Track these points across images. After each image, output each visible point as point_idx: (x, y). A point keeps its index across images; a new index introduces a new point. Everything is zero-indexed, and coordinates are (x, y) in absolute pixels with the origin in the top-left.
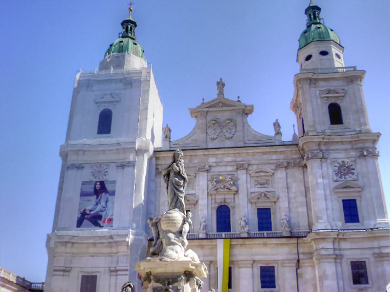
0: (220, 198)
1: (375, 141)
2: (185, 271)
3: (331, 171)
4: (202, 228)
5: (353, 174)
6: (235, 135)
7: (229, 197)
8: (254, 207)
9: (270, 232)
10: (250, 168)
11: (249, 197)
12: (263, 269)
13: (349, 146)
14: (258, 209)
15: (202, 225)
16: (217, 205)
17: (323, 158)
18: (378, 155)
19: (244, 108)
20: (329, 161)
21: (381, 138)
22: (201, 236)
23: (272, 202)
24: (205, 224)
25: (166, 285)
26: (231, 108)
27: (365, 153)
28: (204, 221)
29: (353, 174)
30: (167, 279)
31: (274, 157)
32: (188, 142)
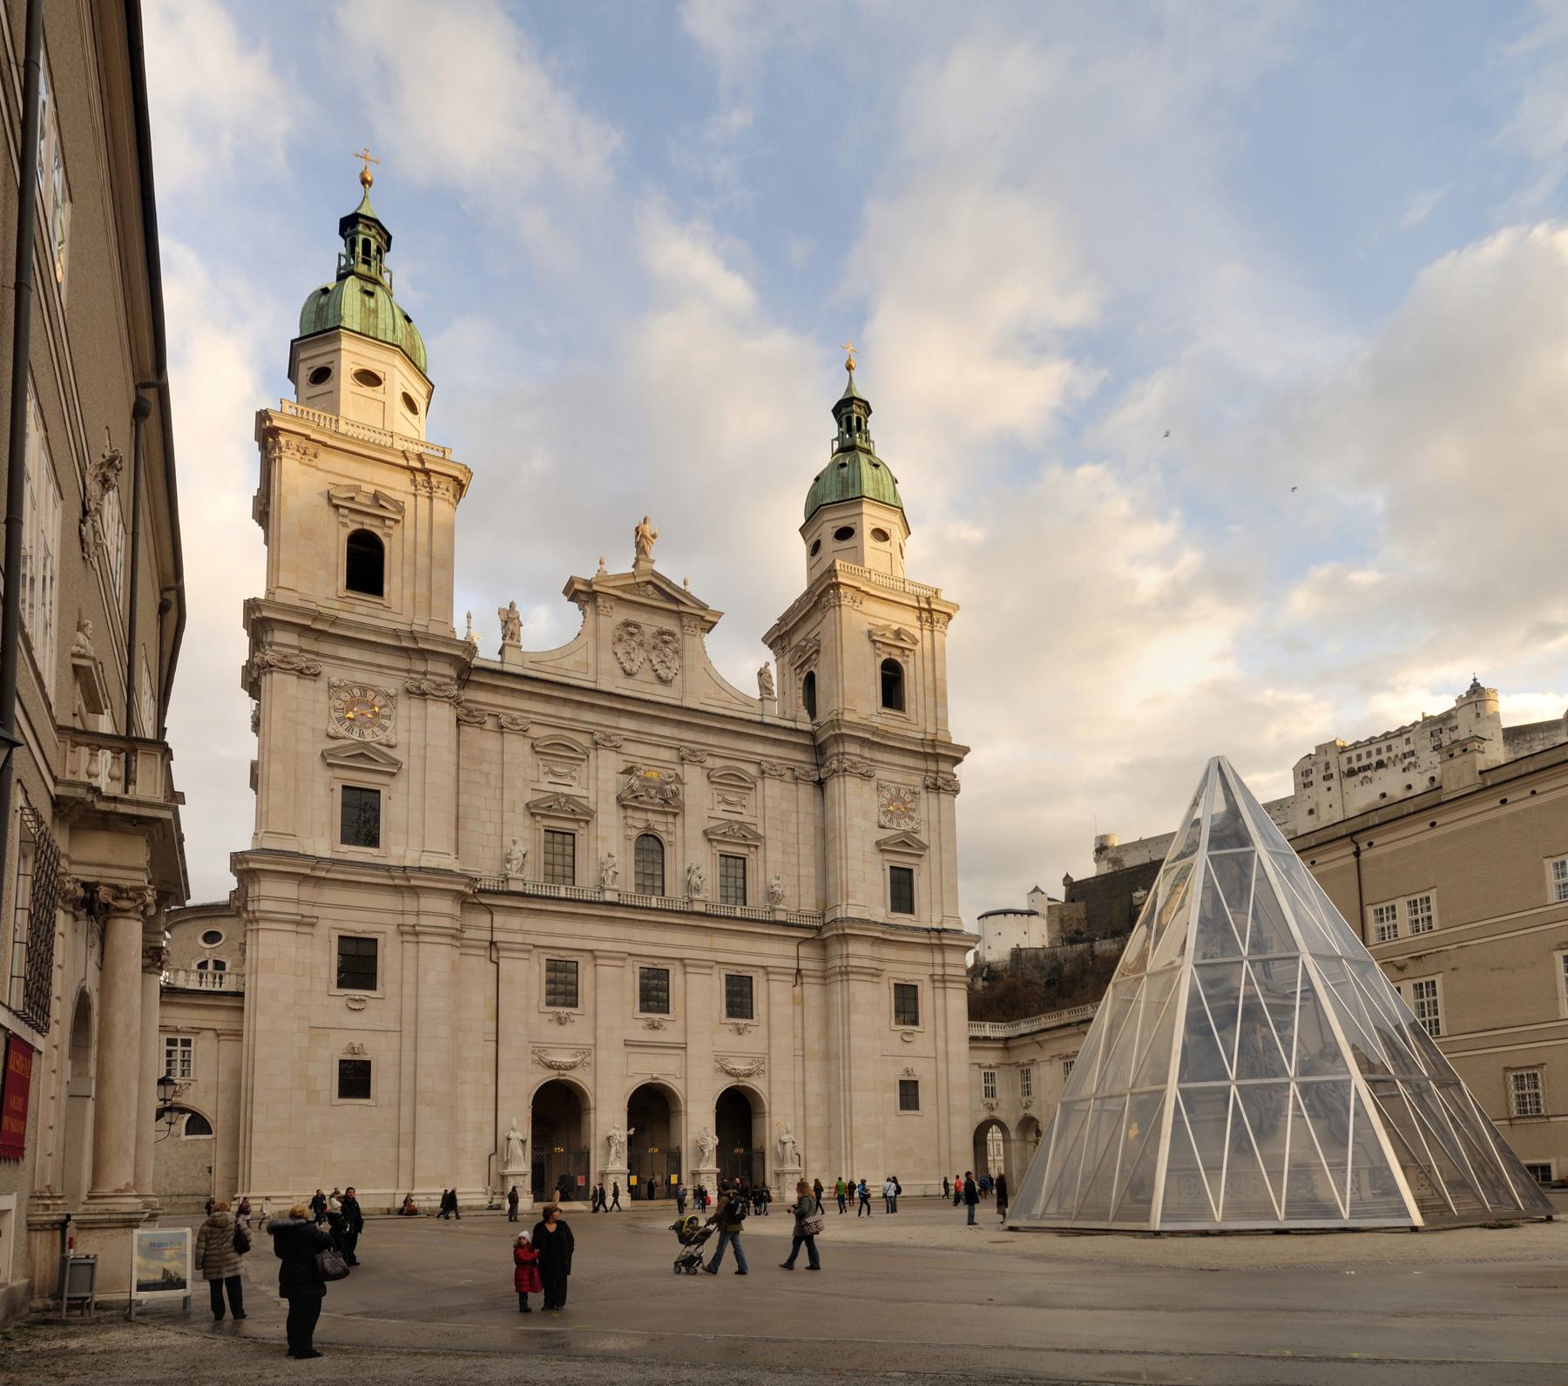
0: (639, 820)
1: (958, 761)
3: (875, 806)
5: (912, 819)
6: (679, 678)
7: (659, 823)
10: (710, 762)
13: (910, 762)
15: (611, 873)
16: (634, 833)
17: (867, 777)
18: (957, 792)
19: (702, 613)
20: (874, 784)
21: (966, 758)
22: (610, 896)
26: (673, 607)
27: (940, 783)
29: (912, 819)
31: (759, 748)
32: (568, 663)
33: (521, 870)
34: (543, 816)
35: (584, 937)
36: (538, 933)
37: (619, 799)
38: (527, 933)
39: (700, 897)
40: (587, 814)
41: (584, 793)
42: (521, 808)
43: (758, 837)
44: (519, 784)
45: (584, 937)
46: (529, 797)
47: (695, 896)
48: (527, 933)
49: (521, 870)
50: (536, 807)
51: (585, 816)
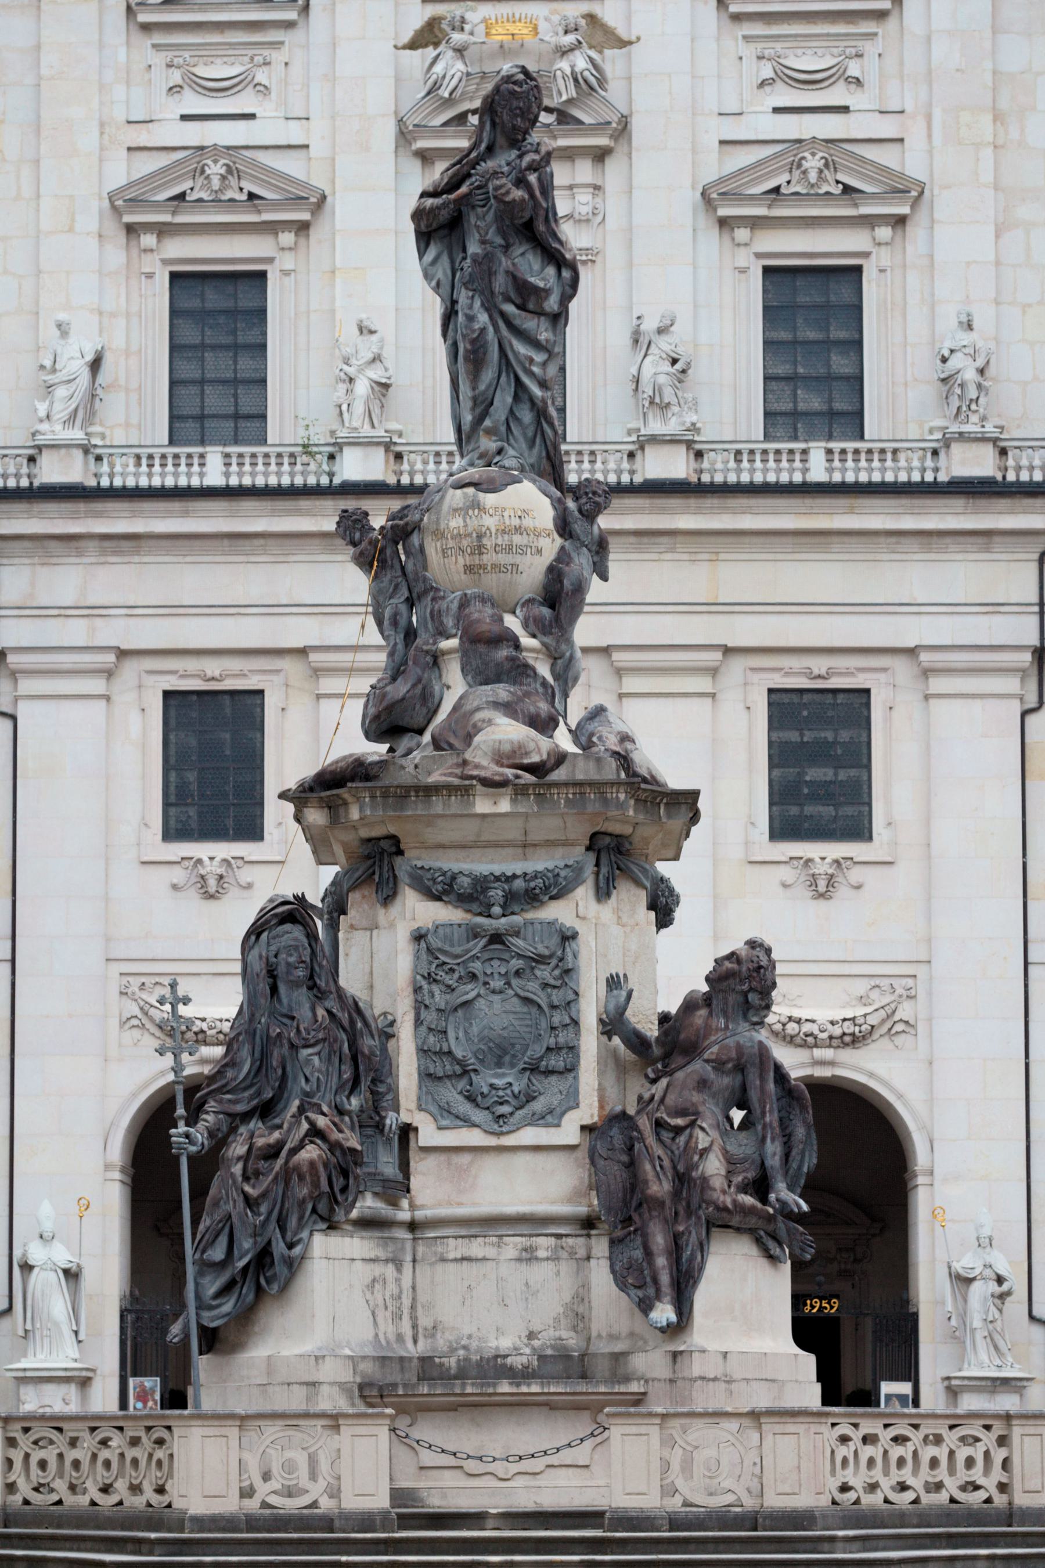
2: (594, 836)
4: (359, 408)
8: (744, 258)
9: (850, 445)
11: (710, 173)
12: (786, 707)
14: (767, 270)
15: (362, 387)
23: (870, 222)
24: (376, 373)
25: (496, 910)
28: (377, 359)
30: (497, 879)
33: (88, 409)
34: (163, 230)
35: (273, 609)
36: (131, 610)
37: (404, 135)
38: (93, 611)
39: (672, 426)
40: (299, 200)
41: (294, 134)
42: (92, 215)
43: (910, 191)
44: (88, 141)
45: (273, 609)
46: (120, 172)
47: (656, 426)
48: (93, 611)
49: (88, 409)
50: (135, 203)
51: (304, 212)
